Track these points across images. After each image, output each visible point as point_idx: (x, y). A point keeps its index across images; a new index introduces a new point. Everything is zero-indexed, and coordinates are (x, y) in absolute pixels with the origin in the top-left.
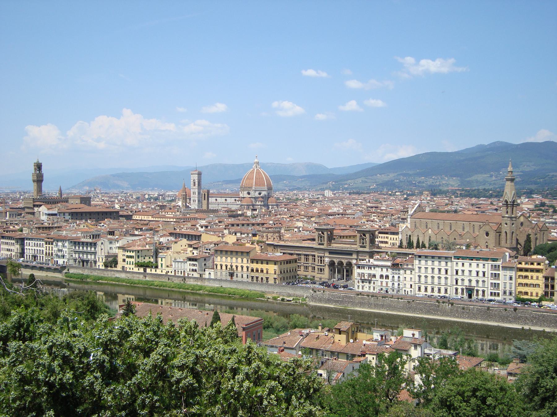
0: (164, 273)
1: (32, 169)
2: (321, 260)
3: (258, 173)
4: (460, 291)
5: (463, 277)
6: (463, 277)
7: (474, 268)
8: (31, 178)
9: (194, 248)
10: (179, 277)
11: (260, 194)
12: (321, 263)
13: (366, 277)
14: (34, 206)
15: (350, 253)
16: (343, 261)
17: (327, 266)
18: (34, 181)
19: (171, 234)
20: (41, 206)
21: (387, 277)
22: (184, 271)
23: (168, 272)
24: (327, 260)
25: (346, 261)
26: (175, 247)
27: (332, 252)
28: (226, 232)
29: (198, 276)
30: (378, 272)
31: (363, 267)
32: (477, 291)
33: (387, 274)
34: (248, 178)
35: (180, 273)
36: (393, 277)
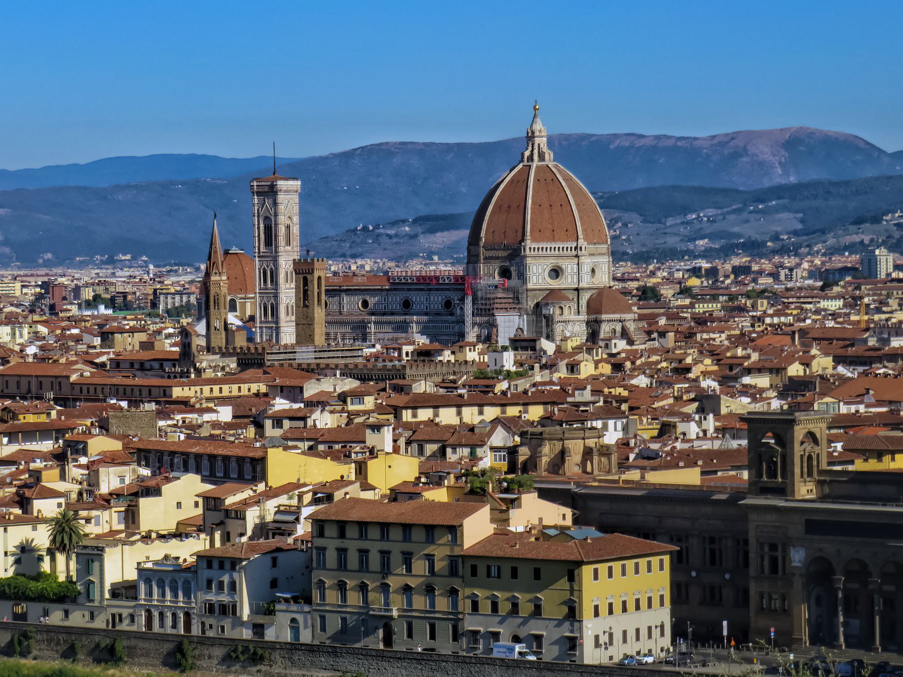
0: (100, 623)
2: (774, 561)
3: (547, 178)
10: (163, 638)
11: (556, 272)
12: (774, 569)
17: (798, 583)
19: (143, 455)
22: (187, 615)
23: (116, 619)
24: (797, 557)
26: (155, 513)
28: (371, 438)
29: (247, 634)
34: (498, 206)
35: (169, 621)
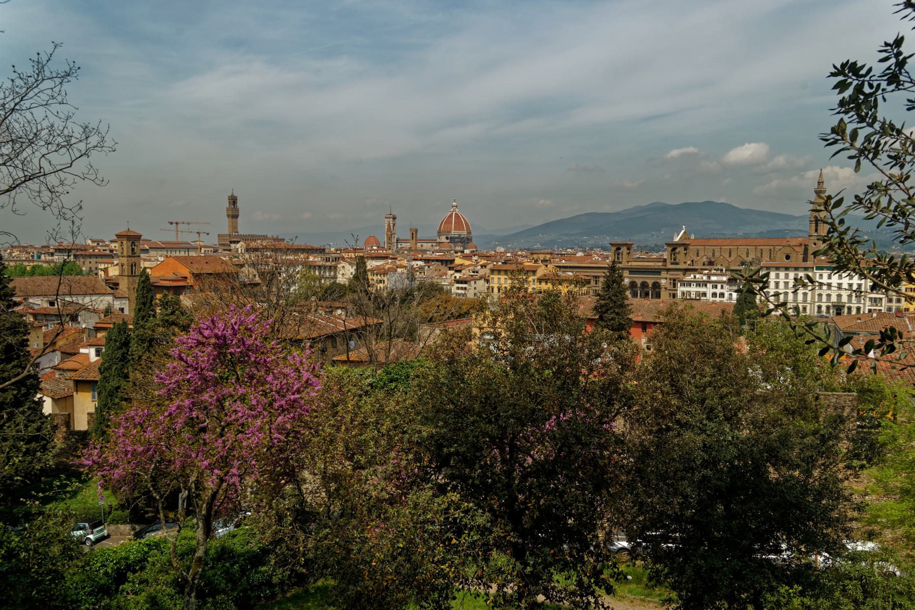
1: (226, 204)
4: (824, 309)
5: (829, 292)
6: (829, 292)
7: (845, 282)
8: (225, 213)
9: (457, 271)
13: (693, 296)
14: (231, 242)
15: (657, 272)
16: (648, 281)
18: (228, 216)
20: (238, 242)
21: (722, 295)
25: (652, 281)
27: (633, 271)
30: (709, 290)
31: (689, 284)
32: (850, 309)
33: (722, 291)
36: (731, 294)
